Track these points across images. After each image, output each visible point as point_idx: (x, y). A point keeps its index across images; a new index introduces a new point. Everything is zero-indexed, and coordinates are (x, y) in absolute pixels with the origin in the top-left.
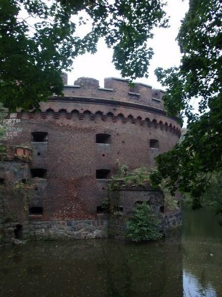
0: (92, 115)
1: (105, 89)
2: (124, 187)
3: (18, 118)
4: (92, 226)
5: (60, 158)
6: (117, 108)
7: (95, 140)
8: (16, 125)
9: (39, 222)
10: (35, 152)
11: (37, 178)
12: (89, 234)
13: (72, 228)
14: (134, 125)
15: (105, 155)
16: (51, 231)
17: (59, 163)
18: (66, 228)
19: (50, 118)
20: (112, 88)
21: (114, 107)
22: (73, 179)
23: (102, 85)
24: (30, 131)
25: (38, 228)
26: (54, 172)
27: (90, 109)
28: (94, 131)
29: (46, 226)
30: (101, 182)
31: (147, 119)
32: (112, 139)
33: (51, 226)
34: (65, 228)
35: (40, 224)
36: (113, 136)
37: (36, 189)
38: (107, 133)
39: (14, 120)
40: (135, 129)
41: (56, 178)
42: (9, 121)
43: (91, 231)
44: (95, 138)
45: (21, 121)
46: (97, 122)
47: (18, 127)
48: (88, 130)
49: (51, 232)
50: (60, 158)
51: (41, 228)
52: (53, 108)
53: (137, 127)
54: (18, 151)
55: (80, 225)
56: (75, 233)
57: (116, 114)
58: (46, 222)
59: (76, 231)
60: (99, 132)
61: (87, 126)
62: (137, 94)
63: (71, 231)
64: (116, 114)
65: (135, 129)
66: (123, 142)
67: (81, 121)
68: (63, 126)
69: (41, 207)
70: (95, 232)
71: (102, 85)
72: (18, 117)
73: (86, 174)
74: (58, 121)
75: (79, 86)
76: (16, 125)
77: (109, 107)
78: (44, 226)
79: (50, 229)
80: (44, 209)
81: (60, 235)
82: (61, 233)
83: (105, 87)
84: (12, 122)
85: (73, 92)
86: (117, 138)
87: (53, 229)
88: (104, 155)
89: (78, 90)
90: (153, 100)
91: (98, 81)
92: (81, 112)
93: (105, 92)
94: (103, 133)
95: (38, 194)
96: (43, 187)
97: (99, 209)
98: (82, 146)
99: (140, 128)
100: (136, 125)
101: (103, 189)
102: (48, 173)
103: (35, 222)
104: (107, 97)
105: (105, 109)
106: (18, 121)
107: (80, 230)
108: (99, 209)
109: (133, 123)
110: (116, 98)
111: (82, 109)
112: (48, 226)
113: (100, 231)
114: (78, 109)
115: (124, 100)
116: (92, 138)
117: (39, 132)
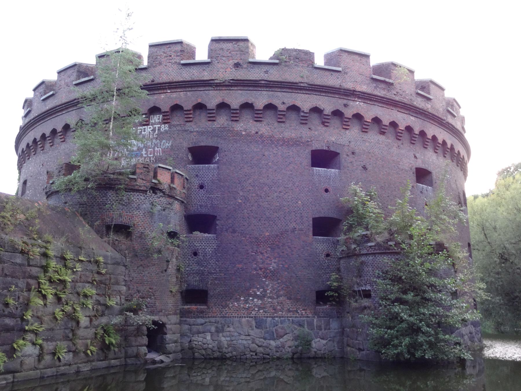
0: (302, 114)
1: (327, 67)
2: (370, 247)
3: (165, 123)
4: (307, 329)
6: (351, 103)
7: (310, 161)
8: (161, 136)
9: (200, 321)
10: (196, 182)
11: (198, 233)
13: (267, 332)
14: (382, 138)
15: (330, 189)
16: (223, 339)
17: (240, 203)
18: (255, 332)
19: (222, 120)
21: (345, 102)
22: (267, 234)
23: (319, 61)
24: (186, 145)
25: (199, 333)
26: (230, 221)
27: (298, 104)
28: (307, 144)
29: (213, 329)
31: (409, 129)
33: (223, 327)
34: (252, 333)
35: (202, 324)
36: (343, 157)
37: (195, 254)
38: (332, 149)
39: (157, 126)
40: (386, 146)
41: (234, 231)
42: (149, 129)
44: (310, 157)
45: (170, 127)
46: (313, 128)
47: (163, 139)
48: (296, 143)
49: (224, 340)
50: (241, 194)
51: (203, 332)
52: (228, 101)
54: (159, 175)
55: (283, 328)
56: (272, 343)
57: (349, 113)
58: (213, 320)
59: (274, 339)
60: (317, 146)
61: (293, 135)
62: (387, 80)
63: (265, 339)
64: (349, 113)
65: (386, 146)
67: (283, 125)
69: (204, 288)
72: (165, 121)
73: (292, 225)
74: (239, 127)
75: (277, 61)
76: (161, 136)
77: (334, 100)
78: (208, 327)
79: (221, 335)
80: (211, 293)
81: (242, 347)
82: (245, 342)
83: (326, 64)
84: (154, 130)
85: (266, 72)
87: (228, 333)
88: (327, 191)
89: (275, 67)
90: (418, 94)
91: (313, 53)
92: (281, 107)
93: (327, 73)
94: (325, 148)
95: (198, 263)
96: (209, 250)
98: (283, 171)
99: (396, 145)
100: (388, 138)
101: (328, 255)
102: (218, 222)
103: (191, 320)
104: (332, 81)
106: (165, 128)
107: (282, 337)
109: (383, 133)
110: (349, 85)
111: (284, 103)
112: (217, 327)
113: (324, 342)
114: (276, 102)
115: (364, 88)
116: (307, 160)
117: (202, 146)
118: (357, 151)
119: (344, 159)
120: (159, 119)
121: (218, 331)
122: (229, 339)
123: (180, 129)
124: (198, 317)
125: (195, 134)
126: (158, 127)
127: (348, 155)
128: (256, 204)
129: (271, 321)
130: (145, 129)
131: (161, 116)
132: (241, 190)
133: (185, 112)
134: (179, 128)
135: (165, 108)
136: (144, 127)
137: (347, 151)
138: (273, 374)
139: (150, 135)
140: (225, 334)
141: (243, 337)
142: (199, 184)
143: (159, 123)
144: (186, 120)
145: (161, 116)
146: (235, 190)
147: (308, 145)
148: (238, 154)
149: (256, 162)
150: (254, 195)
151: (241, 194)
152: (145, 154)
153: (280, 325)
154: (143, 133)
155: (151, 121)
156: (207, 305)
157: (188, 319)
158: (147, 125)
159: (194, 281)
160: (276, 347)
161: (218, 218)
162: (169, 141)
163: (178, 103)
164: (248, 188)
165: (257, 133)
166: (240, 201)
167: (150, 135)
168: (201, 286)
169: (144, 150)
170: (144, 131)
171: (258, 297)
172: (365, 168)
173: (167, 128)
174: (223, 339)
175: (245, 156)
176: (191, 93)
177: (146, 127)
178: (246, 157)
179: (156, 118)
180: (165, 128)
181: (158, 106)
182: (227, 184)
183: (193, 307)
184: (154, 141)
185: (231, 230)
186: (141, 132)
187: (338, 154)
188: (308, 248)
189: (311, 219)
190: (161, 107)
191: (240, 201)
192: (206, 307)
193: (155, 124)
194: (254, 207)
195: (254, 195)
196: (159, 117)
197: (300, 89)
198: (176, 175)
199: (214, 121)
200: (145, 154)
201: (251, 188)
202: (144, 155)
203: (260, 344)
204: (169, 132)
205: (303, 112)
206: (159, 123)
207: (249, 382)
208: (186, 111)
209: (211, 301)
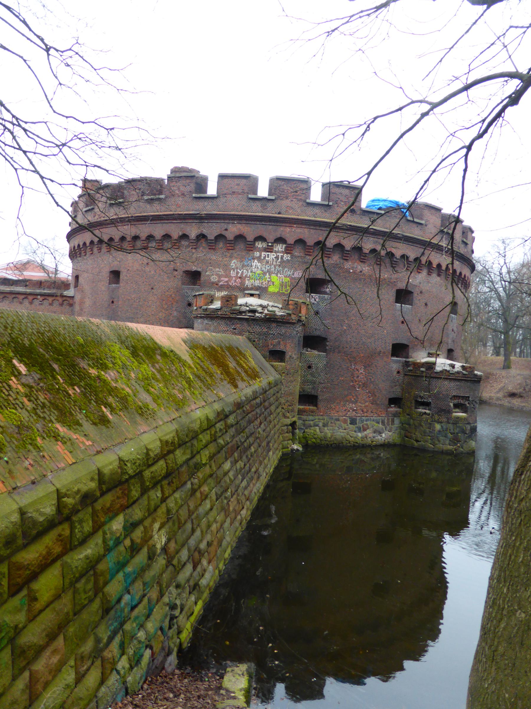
0: (395, 260)
3: (287, 253)
5: (346, 322)
7: (395, 298)
9: (311, 418)
11: (309, 350)
12: (376, 438)
14: (438, 278)
16: (328, 431)
17: (345, 330)
19: (336, 258)
20: (422, 219)
22: (362, 355)
28: (394, 284)
30: (397, 362)
32: (414, 299)
33: (327, 423)
36: (415, 295)
39: (280, 255)
42: (272, 256)
43: (380, 433)
44: (395, 295)
45: (292, 257)
53: (442, 281)
55: (367, 425)
56: (360, 435)
63: (355, 432)
64: (424, 259)
66: (426, 304)
68: (354, 272)
69: (315, 394)
70: (384, 435)
71: (263, 191)
72: (288, 251)
74: (348, 265)
78: (317, 423)
79: (326, 428)
80: (320, 398)
82: (342, 434)
84: (277, 258)
86: (420, 298)
87: (331, 428)
95: (312, 375)
96: (321, 365)
97: (394, 401)
103: (304, 417)
105: (412, 252)
106: (287, 257)
107: (366, 430)
108: (394, 401)
112: (324, 423)
113: (390, 434)
117: (318, 278)
118: (424, 291)
119: (417, 298)
121: (324, 425)
122: (331, 431)
123: (301, 260)
124: (310, 415)
127: (418, 294)
128: (356, 331)
129: (359, 419)
130: (268, 255)
133: (307, 247)
135: (291, 240)
136: (268, 253)
137: (418, 290)
138: (358, 457)
139: (273, 261)
140: (329, 428)
141: (342, 431)
143: (282, 252)
144: (307, 253)
147: (395, 285)
149: (358, 296)
150: (355, 324)
152: (269, 278)
153: (365, 422)
154: (267, 258)
155: (274, 249)
156: (316, 405)
157: (302, 416)
158: (271, 252)
159: (308, 388)
160: (361, 438)
161: (328, 340)
162: (291, 270)
163: (302, 238)
164: (352, 318)
165: (361, 272)
167: (273, 261)
168: (313, 393)
169: (268, 274)
170: (268, 257)
171: (352, 402)
172: (426, 304)
174: (328, 431)
175: (351, 290)
176: (315, 231)
177: (270, 253)
179: (280, 247)
181: (283, 237)
183: (307, 407)
184: (277, 267)
186: (265, 257)
187: (412, 293)
188: (387, 367)
189: (391, 345)
190: (287, 239)
192: (315, 408)
193: (278, 252)
194: (354, 334)
195: (355, 324)
197: (396, 239)
199: (329, 257)
200: (269, 278)
201: (354, 318)
202: (268, 279)
203: (352, 435)
204: (291, 262)
205: (396, 258)
206: (282, 252)
207: (342, 462)
208: (308, 246)
209: (321, 404)
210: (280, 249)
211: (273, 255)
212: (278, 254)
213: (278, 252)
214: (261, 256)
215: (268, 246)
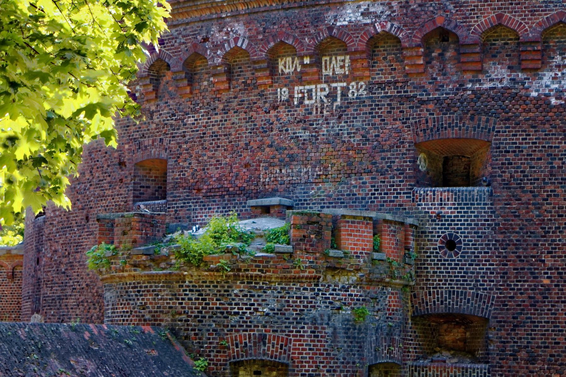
3: (355, 79)
5: (549, 263)
26: (521, 332)
39: (339, 85)
50: (549, 262)
54: (344, 235)
84: (332, 96)
120: (342, 67)
125: (431, 106)
126: (342, 88)
130: (310, 91)
131: (348, 57)
132: (549, 253)
134: (391, 92)
136: (308, 87)
139: (322, 109)
142: (445, 237)
145: (348, 57)
146: (534, 252)
148: (540, 159)
151: (549, 262)
154: (307, 102)
158: (318, 81)
166: (546, 282)
170: (310, 98)
173: (363, 93)
177: (313, 87)
178: (560, 167)
180: (358, 90)
182: (513, 237)
185: (523, 354)
186: (303, 98)
191: (546, 282)
193: (334, 79)
196: (343, 61)
198: (384, 227)
204: (367, 103)
206: (345, 78)
210: (338, 71)
211: (323, 90)
212: (334, 85)
213: (334, 79)
214: (291, 97)
215: (303, 65)
